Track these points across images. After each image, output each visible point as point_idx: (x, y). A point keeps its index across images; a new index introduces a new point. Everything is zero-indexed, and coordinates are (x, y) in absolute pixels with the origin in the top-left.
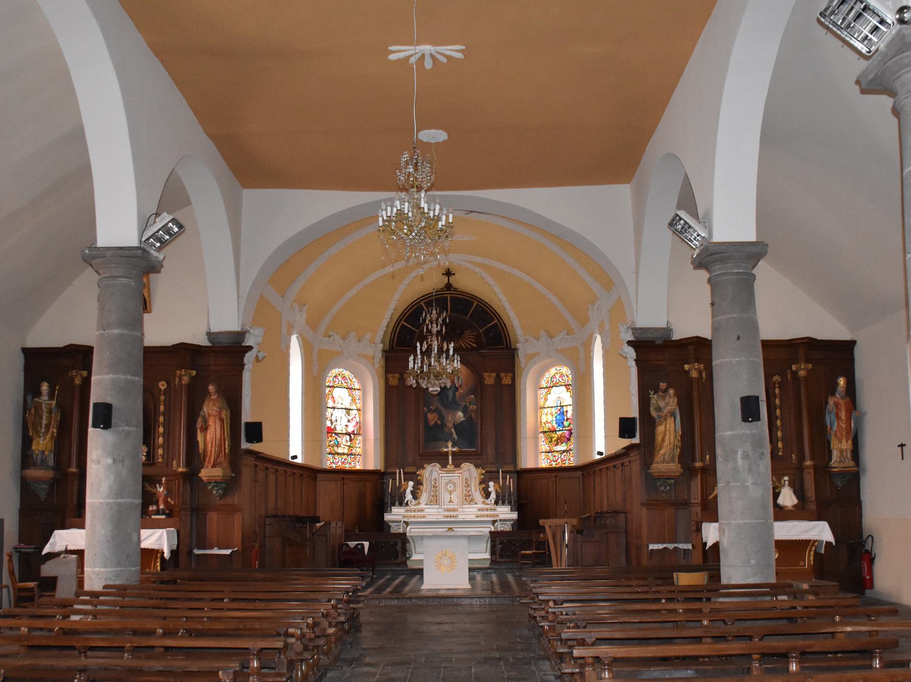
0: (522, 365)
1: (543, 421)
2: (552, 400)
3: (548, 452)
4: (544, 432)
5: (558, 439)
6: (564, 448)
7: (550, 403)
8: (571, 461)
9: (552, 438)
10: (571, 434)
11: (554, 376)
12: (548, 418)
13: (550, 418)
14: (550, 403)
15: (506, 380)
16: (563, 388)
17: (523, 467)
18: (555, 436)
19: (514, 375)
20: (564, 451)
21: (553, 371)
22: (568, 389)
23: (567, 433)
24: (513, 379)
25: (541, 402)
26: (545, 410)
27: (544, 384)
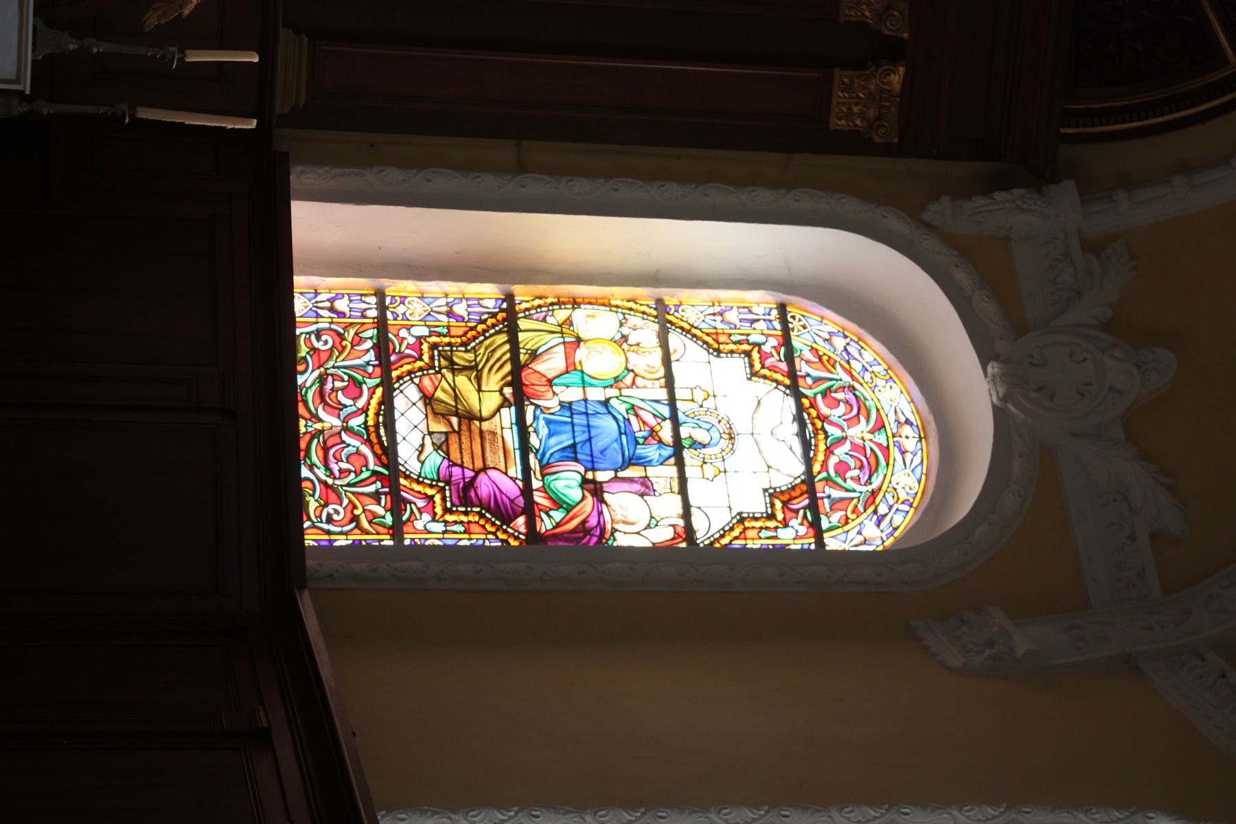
0: (939, 211)
1: (579, 316)
2: (722, 389)
3: (382, 347)
4: (509, 320)
5: (469, 417)
6: (406, 453)
7: (692, 364)
8: (337, 513)
9: (475, 371)
10: (501, 512)
11: (860, 409)
12: (599, 352)
13: (600, 361)
14: (692, 364)
15: (854, 100)
16: (790, 469)
17: (298, 177)
18: (486, 397)
19: (884, 151)
20: (388, 454)
21: (894, 397)
22: (782, 497)
23: (503, 481)
24: (855, 143)
25: (693, 306)
26: (647, 333)
27: (816, 328)
